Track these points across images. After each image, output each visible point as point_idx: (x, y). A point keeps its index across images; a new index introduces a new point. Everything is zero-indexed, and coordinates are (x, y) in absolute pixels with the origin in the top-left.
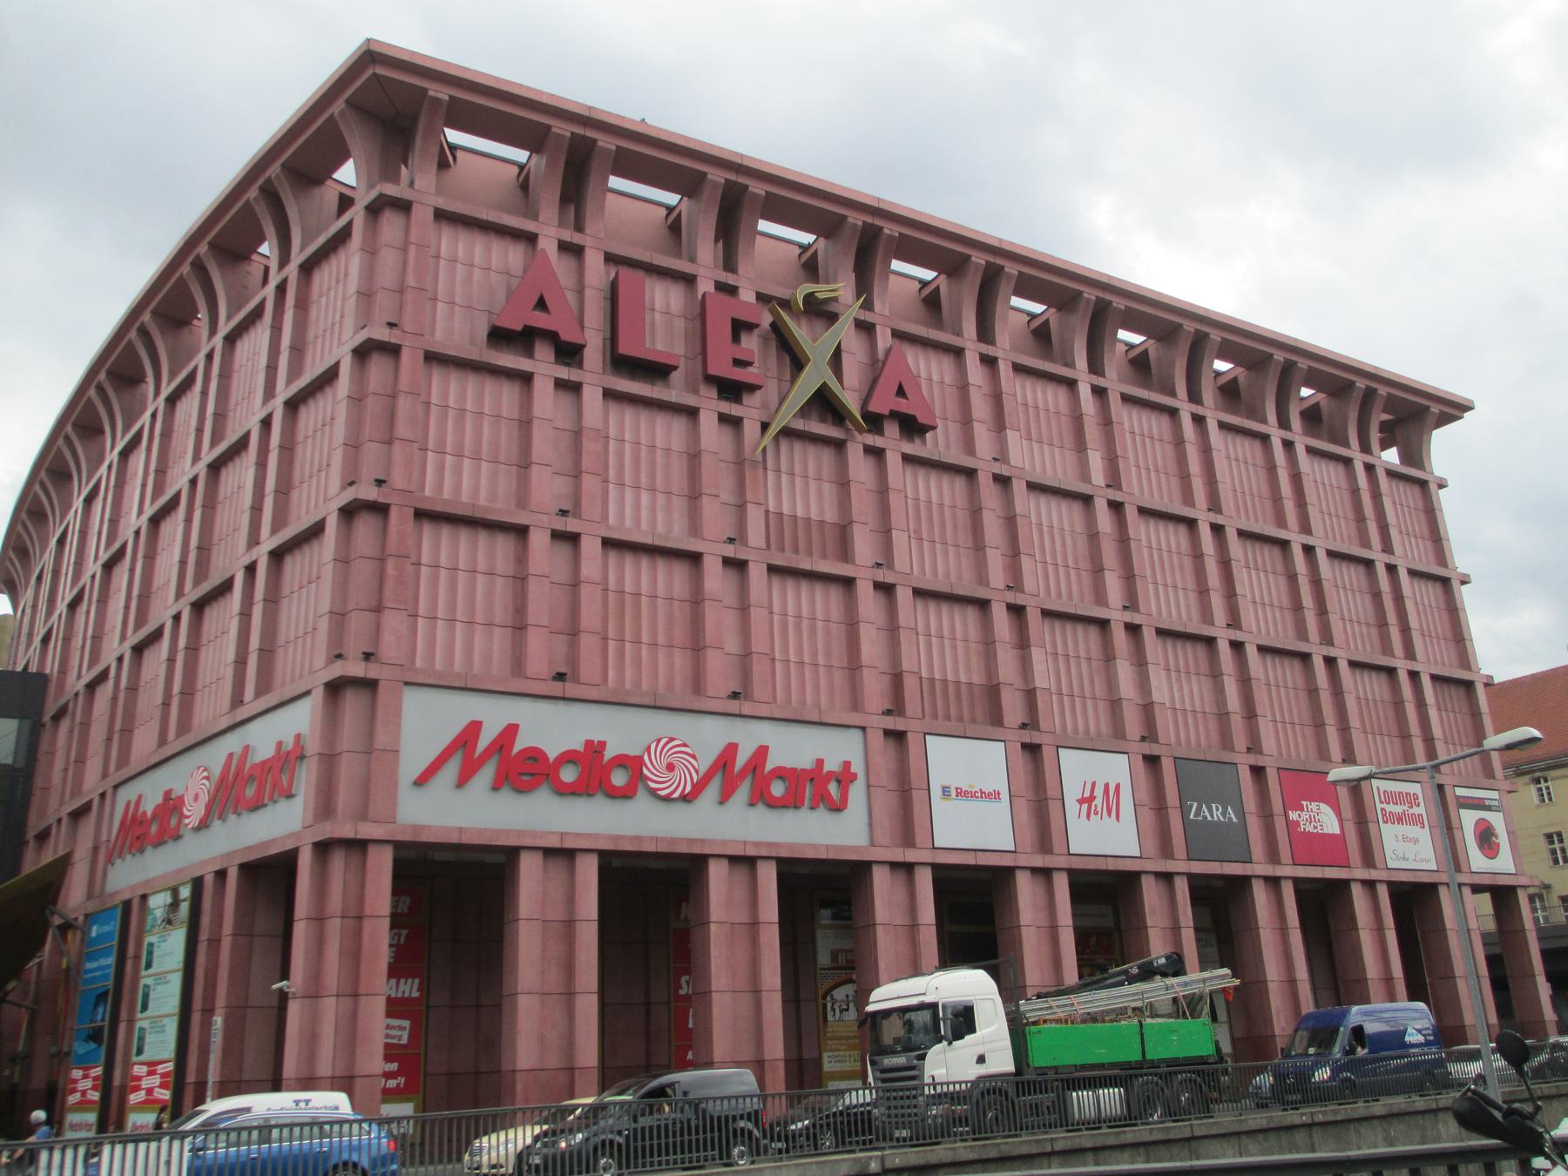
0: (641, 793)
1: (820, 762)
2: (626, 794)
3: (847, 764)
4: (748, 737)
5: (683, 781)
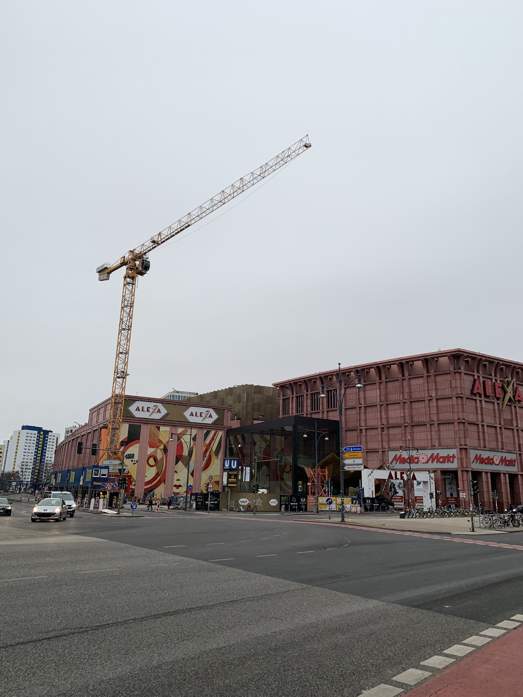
0: (419, 463)
1: (448, 455)
2: (417, 463)
3: (453, 455)
4: (435, 452)
5: (425, 460)
